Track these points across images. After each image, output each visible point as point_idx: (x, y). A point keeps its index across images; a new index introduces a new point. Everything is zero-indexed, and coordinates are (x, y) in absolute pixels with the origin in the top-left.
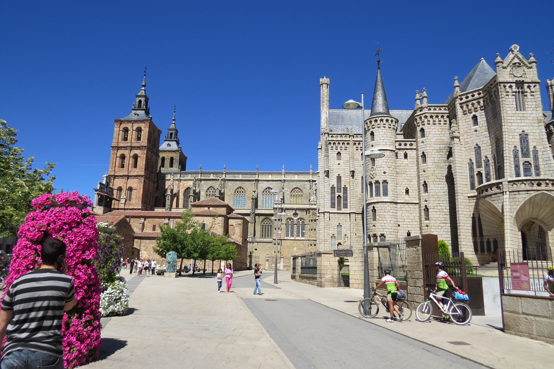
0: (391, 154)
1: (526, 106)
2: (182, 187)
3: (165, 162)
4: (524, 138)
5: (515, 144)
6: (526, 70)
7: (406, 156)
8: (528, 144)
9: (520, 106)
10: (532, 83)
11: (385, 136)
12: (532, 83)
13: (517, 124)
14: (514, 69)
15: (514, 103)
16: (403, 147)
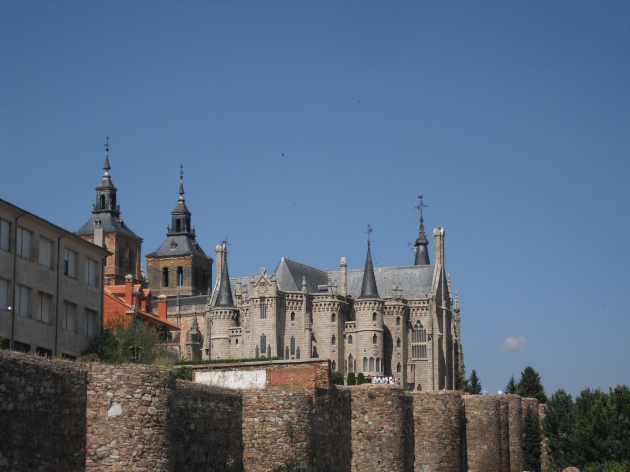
0: (224, 341)
1: (267, 315)
2: (184, 328)
3: (170, 277)
4: (263, 339)
5: (257, 344)
6: (268, 287)
7: (237, 341)
8: (265, 344)
9: (263, 315)
10: (270, 297)
11: (220, 326)
12: (270, 297)
13: (259, 329)
14: (261, 287)
15: (259, 313)
16: (235, 334)
